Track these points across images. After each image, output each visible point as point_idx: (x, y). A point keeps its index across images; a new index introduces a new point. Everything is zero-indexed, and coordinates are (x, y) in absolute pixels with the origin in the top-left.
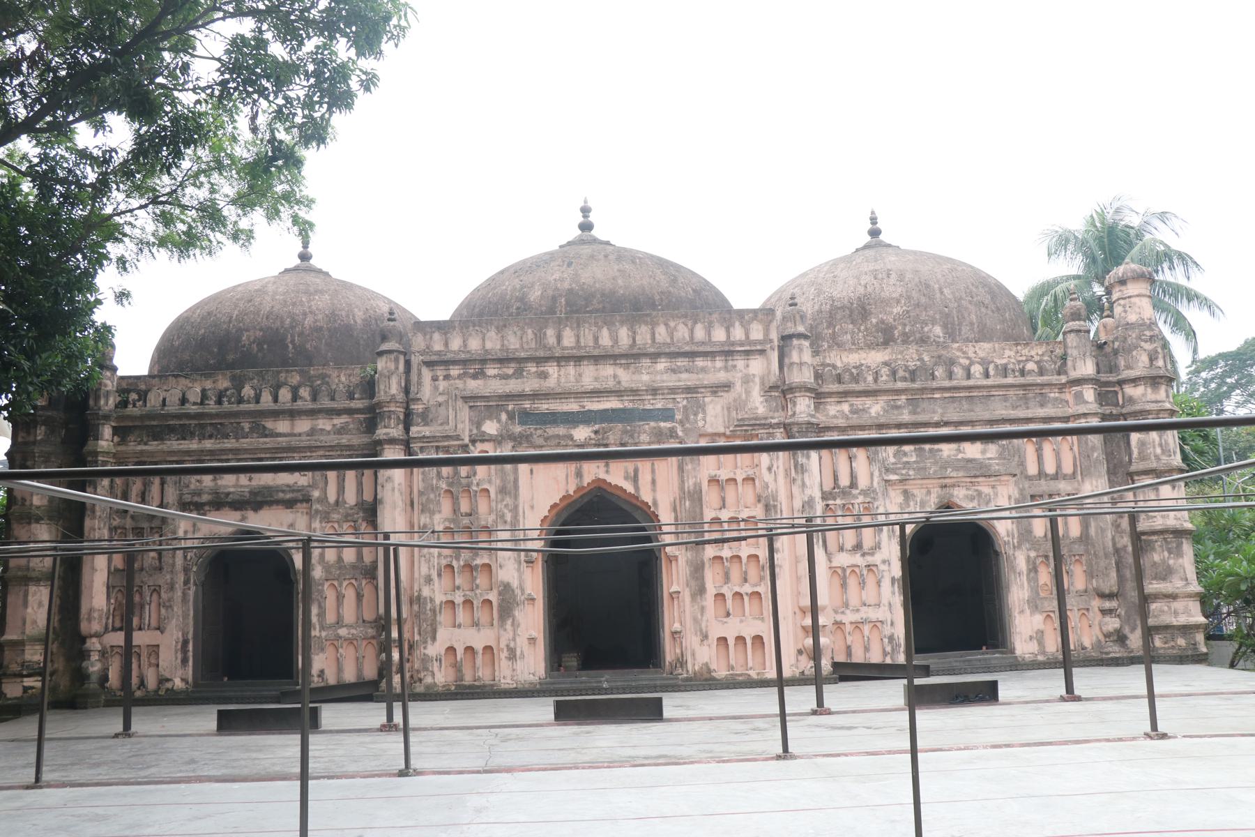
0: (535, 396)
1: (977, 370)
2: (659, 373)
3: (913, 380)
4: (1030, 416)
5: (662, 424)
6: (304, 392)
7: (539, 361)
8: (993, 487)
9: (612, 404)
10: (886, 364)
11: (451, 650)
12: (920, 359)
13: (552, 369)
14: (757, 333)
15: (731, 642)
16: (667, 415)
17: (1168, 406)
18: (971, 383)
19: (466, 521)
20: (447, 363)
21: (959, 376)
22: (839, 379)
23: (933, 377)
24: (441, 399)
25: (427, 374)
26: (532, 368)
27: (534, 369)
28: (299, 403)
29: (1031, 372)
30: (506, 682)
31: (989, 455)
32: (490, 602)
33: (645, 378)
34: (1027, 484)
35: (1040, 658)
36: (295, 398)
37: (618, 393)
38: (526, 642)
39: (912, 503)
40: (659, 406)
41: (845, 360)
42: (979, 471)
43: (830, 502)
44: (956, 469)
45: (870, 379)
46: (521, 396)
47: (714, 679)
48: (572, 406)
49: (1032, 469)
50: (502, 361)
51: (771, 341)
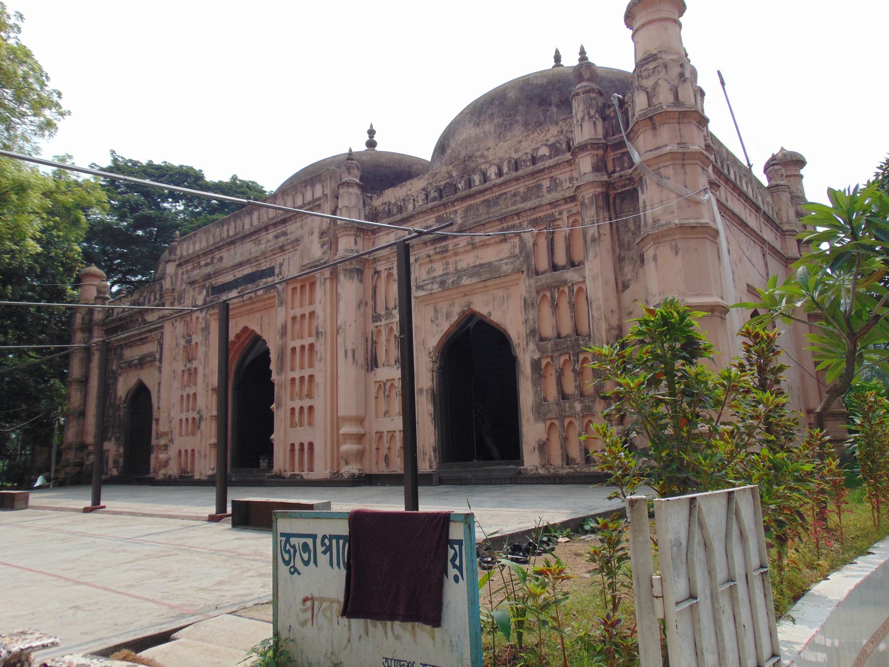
0: (217, 273)
1: (492, 172)
2: (268, 239)
3: (441, 197)
4: (537, 204)
5: (270, 279)
6: (158, 296)
7: (219, 248)
8: (506, 288)
9: (247, 270)
10: (423, 189)
11: (180, 451)
12: (451, 176)
13: (224, 253)
14: (318, 193)
15: (297, 447)
16: (270, 272)
17: (668, 149)
18: (487, 185)
19: (189, 366)
20: (187, 262)
21: (477, 183)
22: (389, 213)
23: (456, 189)
24: (184, 286)
25: (180, 271)
26: (217, 255)
27: (218, 256)
28: (157, 302)
29: (543, 158)
30: (197, 476)
31: (503, 256)
32: (194, 419)
33: (263, 246)
34: (533, 282)
35: (541, 471)
36: (155, 299)
37: (248, 262)
38: (208, 447)
39: (439, 316)
40: (268, 266)
41: (397, 196)
42: (488, 273)
43: (378, 324)
44: (471, 276)
45: (410, 207)
46: (209, 276)
47: (284, 478)
48: (229, 278)
49: (543, 263)
50: (205, 254)
51: (326, 195)
